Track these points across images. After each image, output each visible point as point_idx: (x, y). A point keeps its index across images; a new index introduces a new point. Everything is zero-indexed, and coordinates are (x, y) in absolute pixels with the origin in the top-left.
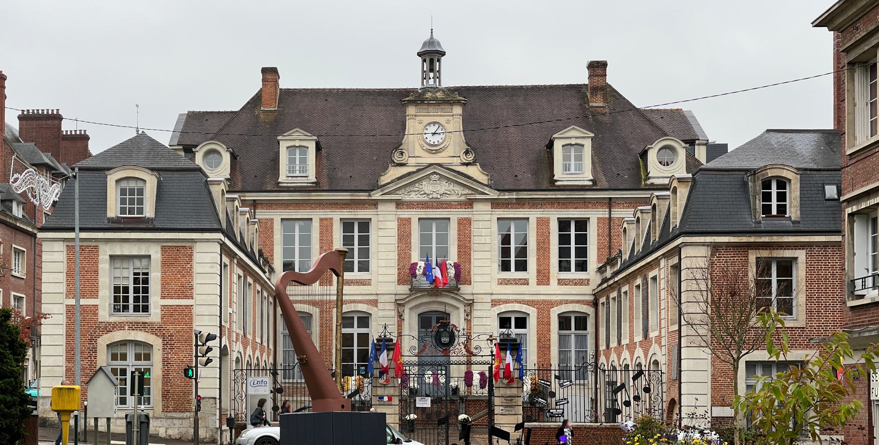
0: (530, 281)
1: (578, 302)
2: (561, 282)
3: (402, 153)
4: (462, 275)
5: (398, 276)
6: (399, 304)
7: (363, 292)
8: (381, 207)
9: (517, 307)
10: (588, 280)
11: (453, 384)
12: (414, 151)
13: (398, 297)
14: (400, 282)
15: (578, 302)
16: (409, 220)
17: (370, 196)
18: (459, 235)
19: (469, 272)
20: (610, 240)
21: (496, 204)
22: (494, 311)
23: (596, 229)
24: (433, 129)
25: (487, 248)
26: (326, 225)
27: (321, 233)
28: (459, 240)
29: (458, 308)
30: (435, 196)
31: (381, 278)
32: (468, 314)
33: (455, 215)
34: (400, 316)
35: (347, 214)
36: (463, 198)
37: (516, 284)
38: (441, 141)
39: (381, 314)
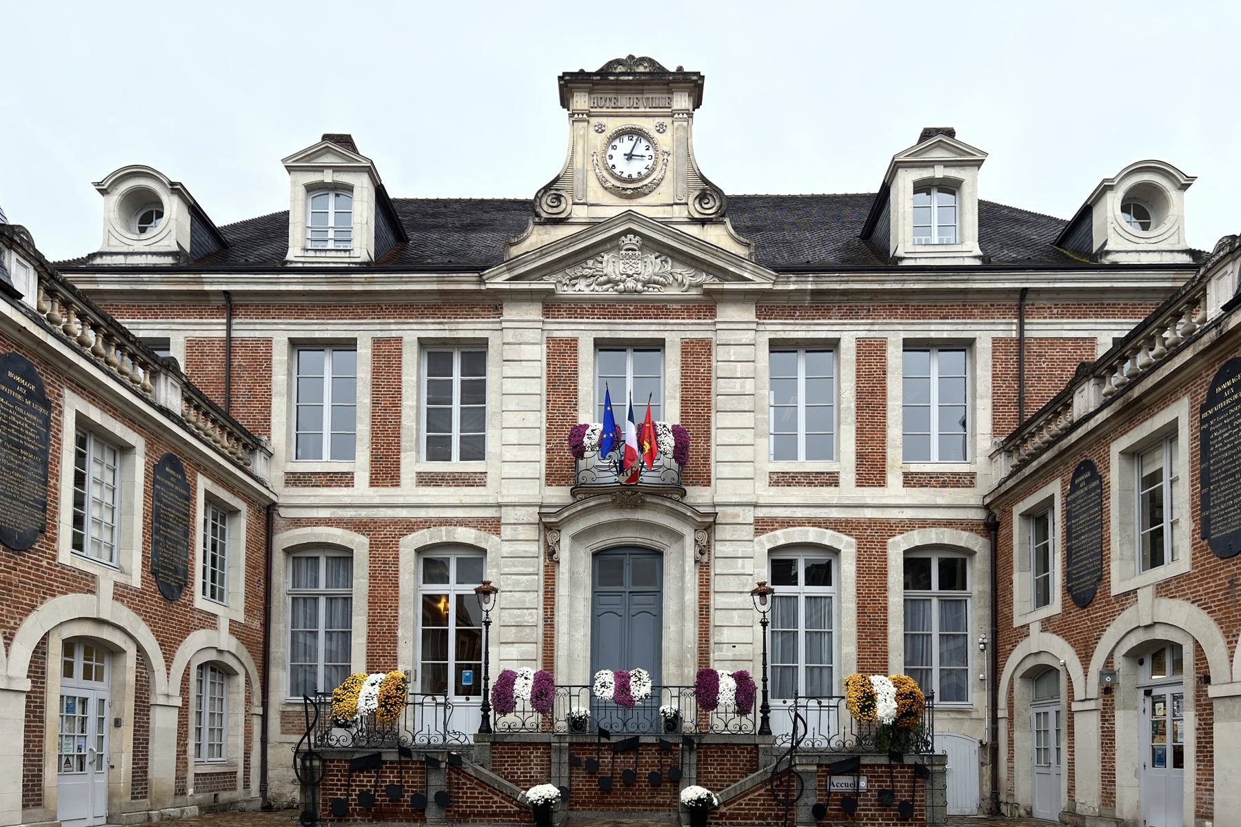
0: (843, 478)
1: (949, 523)
2: (911, 480)
3: (558, 198)
5: (548, 466)
7: (467, 500)
8: (511, 313)
9: (812, 535)
10: (972, 475)
11: (668, 706)
12: (585, 190)
13: (544, 510)
14: (553, 478)
15: (949, 523)
16: (572, 344)
17: (482, 281)
18: (684, 376)
19: (707, 458)
20: (1021, 386)
21: (767, 305)
22: (761, 543)
23: (990, 363)
24: (625, 145)
25: (746, 403)
27: (376, 371)
28: (685, 387)
29: (679, 537)
30: (630, 284)
31: (508, 470)
32: (704, 550)
33: (674, 333)
34: (551, 553)
35: (433, 329)
36: (694, 292)
37: (810, 484)
38: (644, 172)
39: (507, 549)
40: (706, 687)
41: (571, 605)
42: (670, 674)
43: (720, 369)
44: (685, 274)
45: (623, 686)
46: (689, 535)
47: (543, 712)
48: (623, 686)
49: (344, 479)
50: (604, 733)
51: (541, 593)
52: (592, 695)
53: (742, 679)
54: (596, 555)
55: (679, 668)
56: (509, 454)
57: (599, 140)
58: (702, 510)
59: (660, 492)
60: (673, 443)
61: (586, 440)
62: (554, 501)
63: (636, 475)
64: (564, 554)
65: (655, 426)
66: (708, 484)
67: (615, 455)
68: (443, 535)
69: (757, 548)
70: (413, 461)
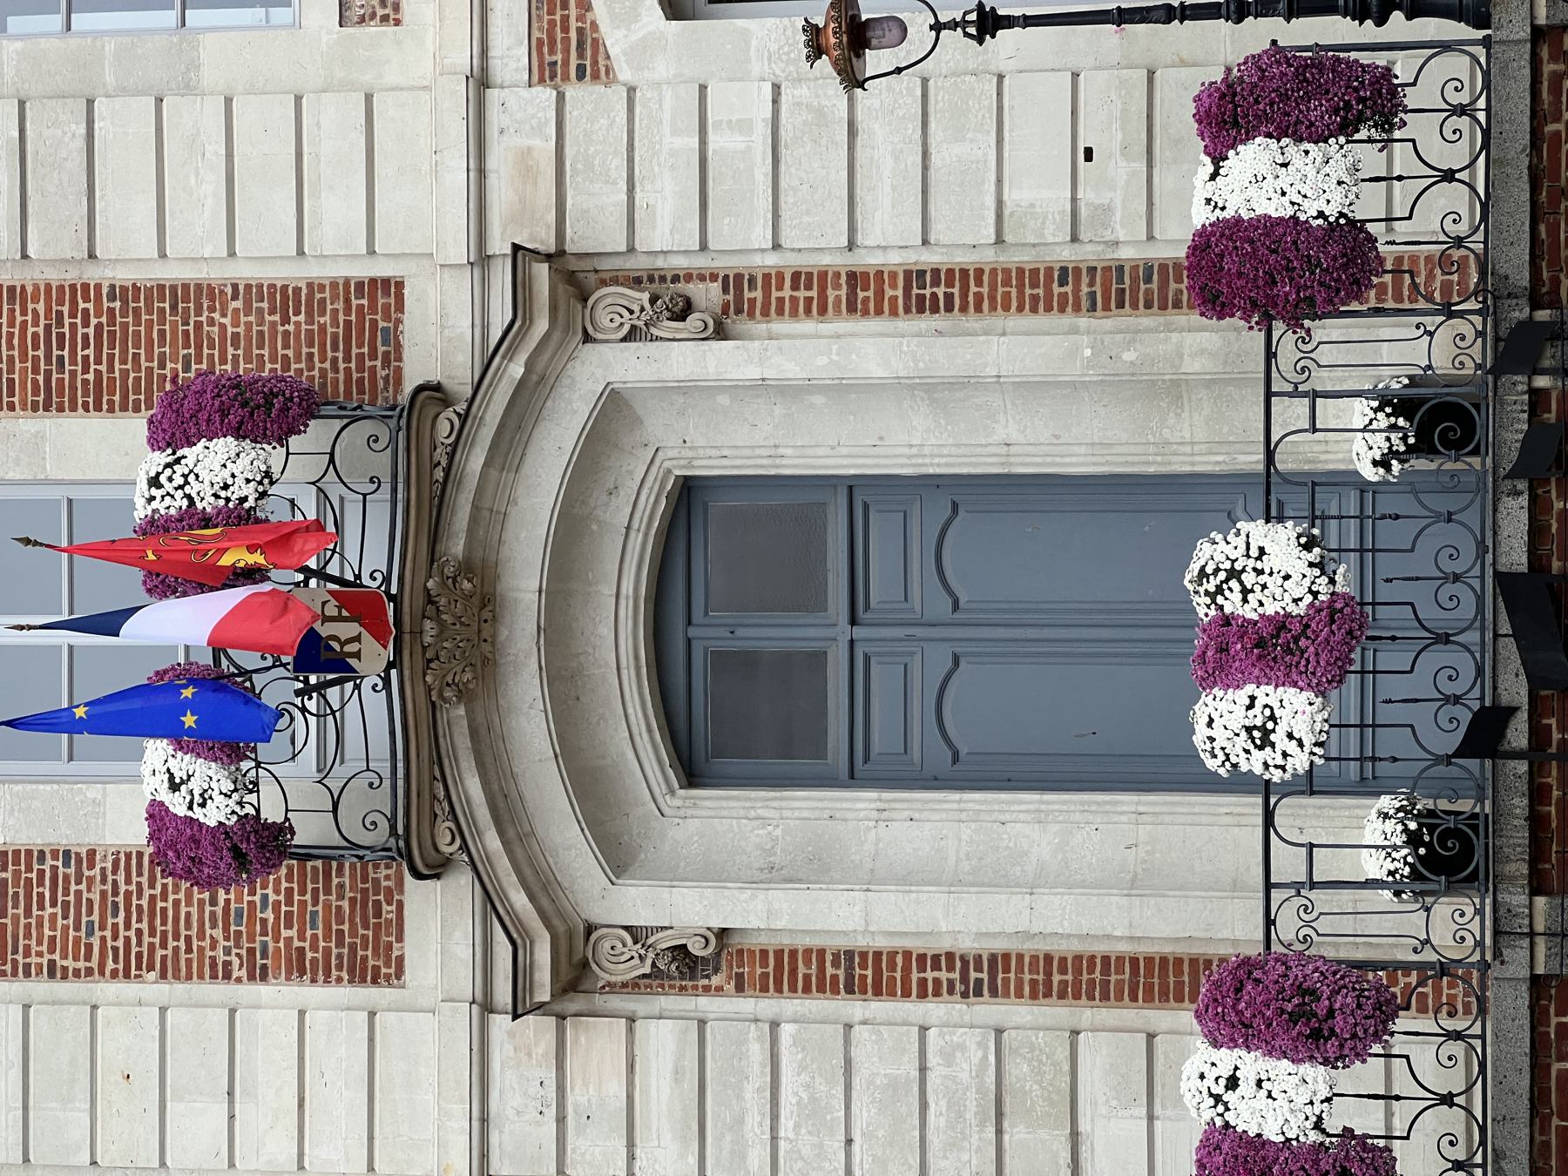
4: (271, 370)
6: (568, 974)
11: (1357, 441)
13: (503, 993)
14: (370, 958)
19: (284, 299)
25: (57, 134)
29: (614, 408)
32: (670, 302)
40: (1269, 277)
41: (907, 879)
42: (1210, 436)
45: (1269, 649)
46: (607, 365)
47: (1384, 1011)
48: (1269, 649)
50: (1484, 735)
51: (855, 1008)
52: (1309, 784)
53: (1228, 117)
54: (691, 773)
55: (1191, 396)
58: (501, 314)
59: (426, 497)
60: (224, 446)
61: (212, 815)
62: (463, 948)
63: (357, 602)
64: (688, 911)
65: (155, 527)
66: (388, 291)
67: (277, 689)
69: (662, 68)
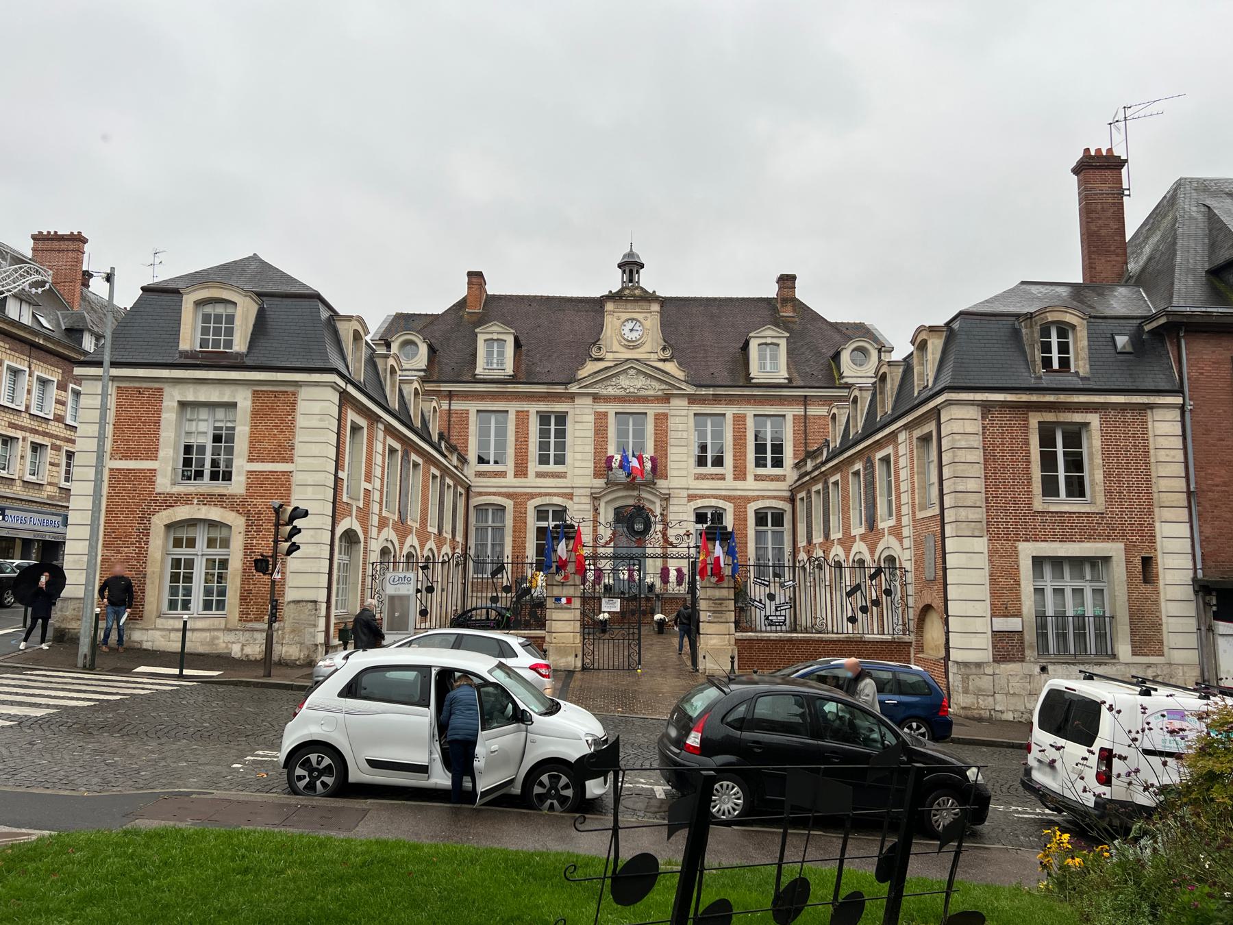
3: (600, 348)
8: (578, 401)
11: (649, 580)
14: (597, 475)
21: (692, 399)
24: (630, 325)
26: (522, 418)
31: (577, 471)
33: (652, 410)
35: (543, 407)
36: (660, 393)
39: (576, 507)
43: (671, 426)
44: (655, 384)
49: (502, 474)
56: (577, 464)
57: (618, 323)
68: (547, 500)
70: (533, 466)
